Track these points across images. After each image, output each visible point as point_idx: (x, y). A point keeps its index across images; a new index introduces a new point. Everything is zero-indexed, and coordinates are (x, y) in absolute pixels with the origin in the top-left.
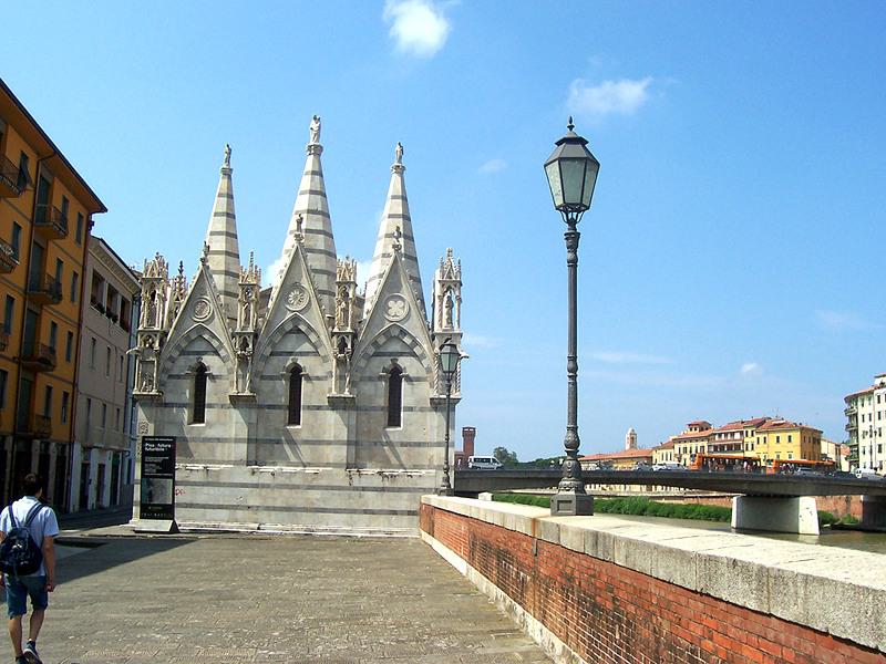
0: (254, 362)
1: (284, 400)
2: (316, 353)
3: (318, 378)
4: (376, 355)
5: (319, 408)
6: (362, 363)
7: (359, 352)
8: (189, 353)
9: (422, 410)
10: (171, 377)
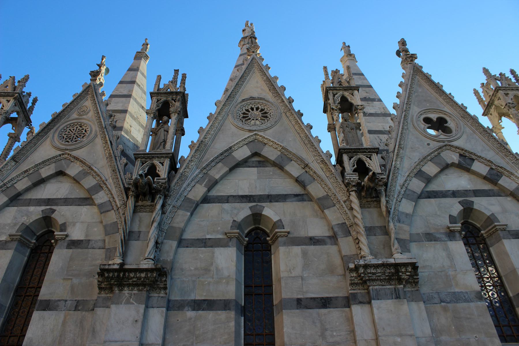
0: (169, 208)
2: (303, 197)
3: (314, 241)
5: (325, 303)
6: (406, 206)
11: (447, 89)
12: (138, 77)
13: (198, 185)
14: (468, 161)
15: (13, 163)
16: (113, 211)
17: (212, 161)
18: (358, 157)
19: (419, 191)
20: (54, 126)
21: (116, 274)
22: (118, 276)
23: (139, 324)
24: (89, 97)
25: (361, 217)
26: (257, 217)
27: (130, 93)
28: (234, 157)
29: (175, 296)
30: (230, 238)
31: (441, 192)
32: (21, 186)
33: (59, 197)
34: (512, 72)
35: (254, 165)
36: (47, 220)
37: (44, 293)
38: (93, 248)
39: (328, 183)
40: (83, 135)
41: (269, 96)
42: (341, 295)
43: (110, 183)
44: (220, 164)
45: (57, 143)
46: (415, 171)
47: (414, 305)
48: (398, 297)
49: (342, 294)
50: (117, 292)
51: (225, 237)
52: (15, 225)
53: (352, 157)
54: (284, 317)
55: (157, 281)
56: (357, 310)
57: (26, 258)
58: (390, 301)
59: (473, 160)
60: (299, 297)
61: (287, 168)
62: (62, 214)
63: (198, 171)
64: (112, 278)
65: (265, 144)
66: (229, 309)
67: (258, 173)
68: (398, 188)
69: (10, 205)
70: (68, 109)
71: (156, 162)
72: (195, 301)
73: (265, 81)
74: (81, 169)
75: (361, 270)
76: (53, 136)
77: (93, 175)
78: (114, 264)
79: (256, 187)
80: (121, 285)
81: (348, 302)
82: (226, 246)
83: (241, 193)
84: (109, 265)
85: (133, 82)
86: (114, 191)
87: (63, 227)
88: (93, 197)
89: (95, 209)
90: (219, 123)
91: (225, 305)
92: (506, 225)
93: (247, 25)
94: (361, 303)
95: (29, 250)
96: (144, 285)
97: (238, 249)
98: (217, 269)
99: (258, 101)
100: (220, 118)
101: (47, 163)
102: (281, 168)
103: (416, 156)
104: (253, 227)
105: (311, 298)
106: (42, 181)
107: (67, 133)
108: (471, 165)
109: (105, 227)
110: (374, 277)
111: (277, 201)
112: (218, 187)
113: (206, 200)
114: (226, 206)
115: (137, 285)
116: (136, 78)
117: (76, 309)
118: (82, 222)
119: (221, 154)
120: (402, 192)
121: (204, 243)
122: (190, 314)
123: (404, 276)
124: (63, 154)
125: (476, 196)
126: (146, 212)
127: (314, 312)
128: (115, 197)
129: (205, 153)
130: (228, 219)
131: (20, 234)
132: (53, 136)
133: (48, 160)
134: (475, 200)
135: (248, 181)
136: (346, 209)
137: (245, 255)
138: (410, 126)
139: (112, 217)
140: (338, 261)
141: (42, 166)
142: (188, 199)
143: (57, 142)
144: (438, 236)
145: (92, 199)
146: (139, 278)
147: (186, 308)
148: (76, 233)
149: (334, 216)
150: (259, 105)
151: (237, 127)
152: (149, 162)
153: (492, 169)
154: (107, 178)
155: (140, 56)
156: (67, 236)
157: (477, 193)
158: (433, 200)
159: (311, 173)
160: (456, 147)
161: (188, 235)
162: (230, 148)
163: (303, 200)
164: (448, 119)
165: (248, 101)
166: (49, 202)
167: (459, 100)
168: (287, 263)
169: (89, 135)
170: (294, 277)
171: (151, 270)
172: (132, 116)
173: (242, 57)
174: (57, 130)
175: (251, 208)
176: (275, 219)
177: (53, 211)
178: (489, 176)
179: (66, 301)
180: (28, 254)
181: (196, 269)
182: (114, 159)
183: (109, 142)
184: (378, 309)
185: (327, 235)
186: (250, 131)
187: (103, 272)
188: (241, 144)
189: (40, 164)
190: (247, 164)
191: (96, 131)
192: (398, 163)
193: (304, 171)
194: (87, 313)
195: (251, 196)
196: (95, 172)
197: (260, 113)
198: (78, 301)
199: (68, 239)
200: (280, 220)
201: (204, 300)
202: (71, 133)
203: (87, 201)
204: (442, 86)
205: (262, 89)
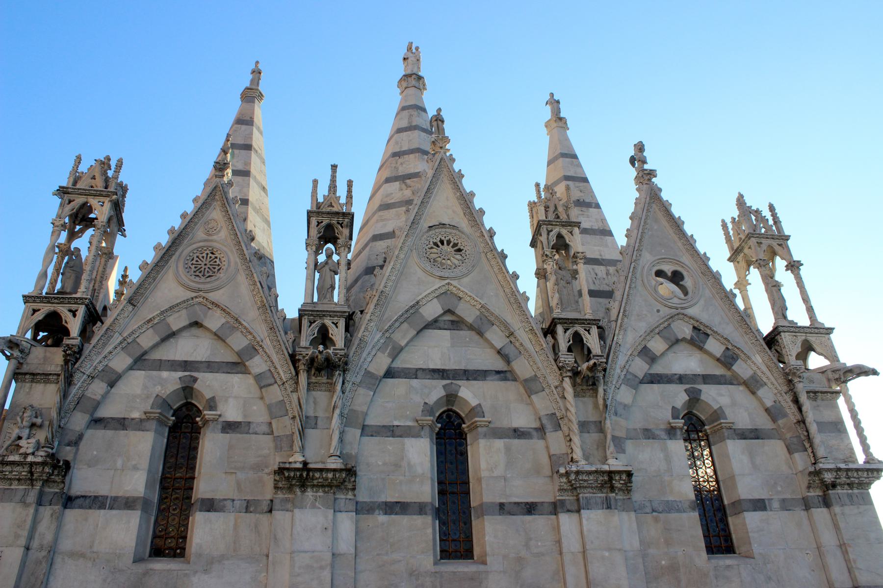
0: (348, 386)
1: (425, 490)
2: (504, 375)
3: (518, 433)
4: (654, 379)
5: (530, 508)
6: (624, 395)
7: (616, 370)
8: (161, 365)
9: (785, 505)
10: (97, 422)
11: (688, 229)
12: (254, 139)
13: (379, 354)
14: (702, 336)
15: (130, 308)
16: (276, 385)
17: (396, 321)
18: (575, 329)
19: (641, 375)
20: (176, 250)
21: (298, 474)
22: (301, 475)
23: (330, 532)
24: (217, 204)
25: (576, 408)
26: (451, 397)
27: (247, 168)
28: (423, 316)
29: (363, 496)
30: (422, 427)
31: (666, 376)
32: (147, 340)
33: (199, 359)
34: (772, 208)
35: (446, 327)
36: (188, 390)
37: (203, 488)
38: (256, 434)
39: (538, 360)
40: (217, 268)
41: (464, 224)
42: (547, 500)
43: (267, 344)
44: (405, 325)
45: (185, 279)
46: (640, 348)
47: (624, 515)
48: (609, 507)
49: (549, 499)
50: (299, 493)
51: (416, 424)
52: (148, 397)
53: (568, 329)
54: (486, 523)
55: (344, 481)
56: (566, 520)
57: (165, 440)
58: (600, 511)
59: (708, 335)
60: (502, 501)
61: (488, 335)
62: (208, 384)
63: (379, 335)
64: (294, 478)
65: (460, 298)
66: (426, 514)
67: (452, 338)
68: (618, 371)
69: (135, 367)
70: (191, 222)
71: (328, 322)
72: (386, 503)
73: (458, 199)
74: (223, 321)
75: (573, 477)
76: (177, 267)
77: (242, 332)
78: (295, 462)
79: (450, 358)
80: (303, 486)
81: (556, 508)
82: (417, 436)
83: (432, 367)
84: (290, 463)
85: (248, 147)
86: (275, 358)
87: (212, 404)
88: (247, 363)
89: (250, 380)
90: (401, 263)
91: (421, 509)
92: (733, 423)
93: (409, 49)
94: (569, 511)
95: (167, 430)
96: (330, 486)
97: (431, 439)
98: (409, 464)
99: (450, 231)
100: (402, 256)
101: (176, 309)
102: (480, 334)
103: (642, 327)
104: (445, 408)
105: (515, 503)
106: (173, 334)
107: (194, 262)
108: (704, 343)
109: (269, 407)
110: (585, 484)
111: (475, 379)
112: (403, 355)
113: (390, 374)
114: (415, 382)
115: (323, 486)
116: (251, 138)
117: (247, 510)
118: (236, 397)
119: (407, 311)
120: (622, 377)
121: (391, 431)
122: (382, 518)
123: (617, 485)
124: (196, 297)
125: (705, 383)
126: (321, 390)
127: (519, 519)
128: (278, 367)
129: (386, 308)
130: (418, 400)
131: (159, 411)
132: (177, 267)
133: (177, 305)
134: (704, 388)
135: (438, 350)
136: (557, 396)
137: (438, 444)
138: (639, 282)
139: (275, 393)
140: (545, 460)
141: (169, 313)
142: (369, 372)
143: (183, 277)
144: (657, 432)
145: (245, 365)
146: (327, 479)
147: (377, 512)
148: (231, 412)
149: (543, 404)
150: (450, 237)
151: (425, 271)
152: (318, 322)
153: (727, 348)
154: (262, 337)
155: (251, 95)
156: (220, 416)
157: (707, 379)
158: (655, 386)
159: (517, 344)
160: (690, 318)
161: (371, 421)
162: (418, 303)
163: (506, 379)
164: (685, 273)
165: (437, 230)
166: (186, 365)
167: (701, 247)
168: (486, 458)
169: (227, 269)
170: (497, 477)
171: (341, 470)
172: (255, 209)
173: (406, 113)
174: (180, 256)
175: (444, 387)
176: (474, 402)
177: (195, 380)
178: (723, 359)
179: (233, 500)
180: (166, 434)
181: (385, 464)
182: (269, 311)
183: (258, 284)
184: (587, 520)
185: (534, 426)
186: (441, 278)
187: (281, 471)
188: (431, 297)
189: (166, 311)
190: (437, 324)
191: (236, 263)
192: (621, 337)
193: (508, 340)
194: (261, 516)
195: (443, 371)
196: (245, 328)
197: (453, 250)
198: (248, 501)
199: (221, 419)
200: (479, 405)
201: (397, 502)
202: (200, 262)
203: (238, 366)
204: (683, 223)
205: (454, 212)
